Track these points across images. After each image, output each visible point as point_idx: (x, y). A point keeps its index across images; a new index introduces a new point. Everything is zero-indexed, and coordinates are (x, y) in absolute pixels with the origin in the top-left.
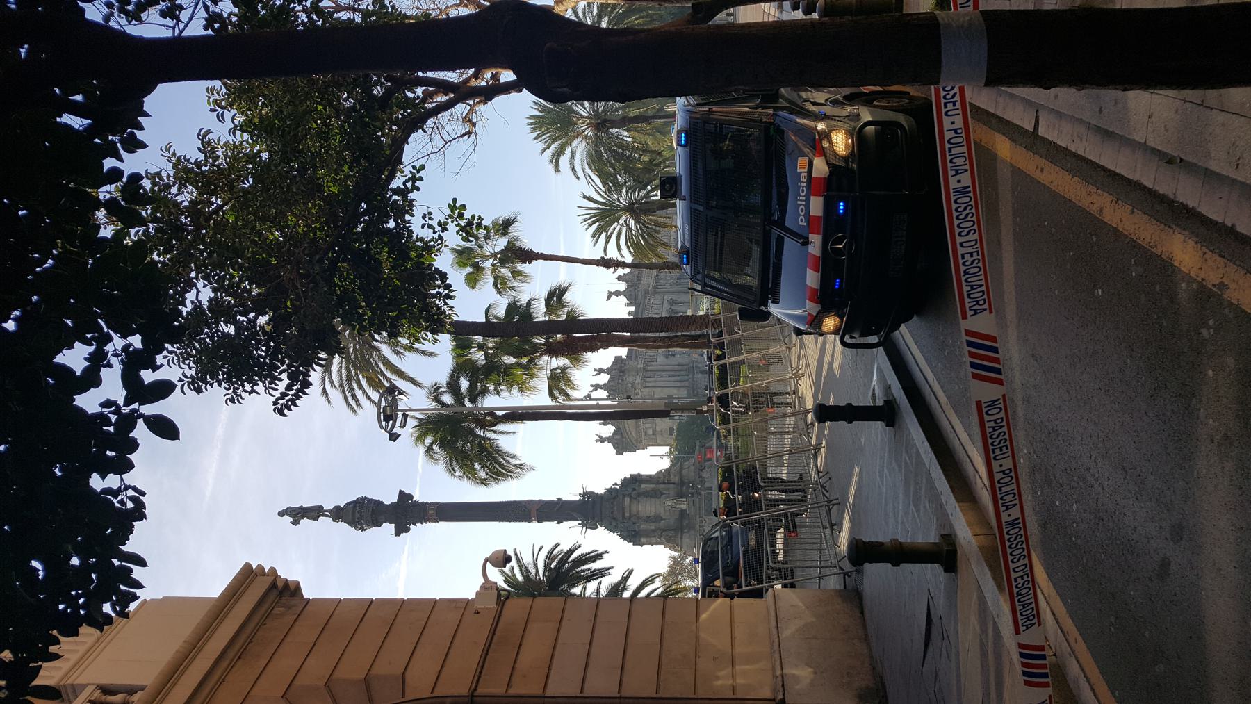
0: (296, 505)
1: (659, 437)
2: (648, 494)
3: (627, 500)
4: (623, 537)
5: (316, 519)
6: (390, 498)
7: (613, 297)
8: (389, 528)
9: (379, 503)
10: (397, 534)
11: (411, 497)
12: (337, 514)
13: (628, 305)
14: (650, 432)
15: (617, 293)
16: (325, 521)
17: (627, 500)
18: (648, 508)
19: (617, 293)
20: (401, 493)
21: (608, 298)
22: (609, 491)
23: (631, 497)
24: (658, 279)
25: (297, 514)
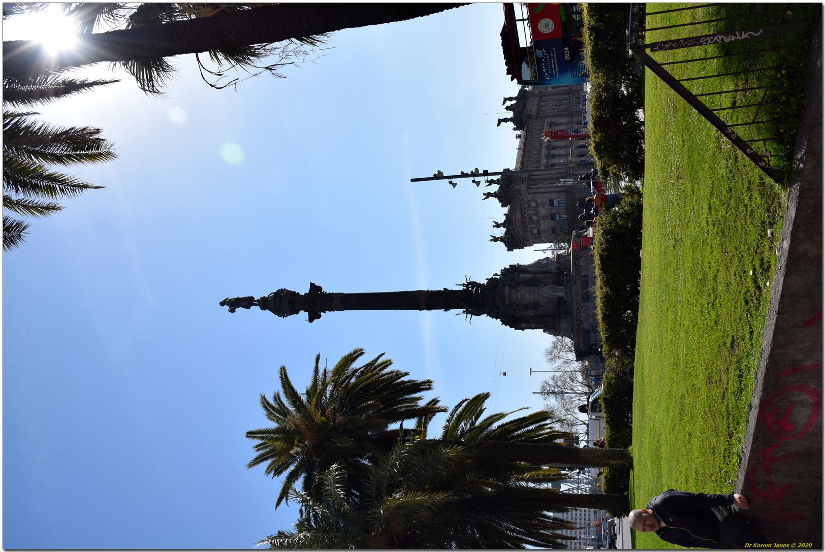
0: (233, 296)
1: (543, 235)
2: (526, 283)
3: (507, 289)
4: (505, 322)
5: (248, 307)
6: (303, 290)
7: (503, 123)
8: (304, 315)
9: (294, 294)
10: (311, 320)
11: (320, 288)
12: (264, 304)
13: (515, 129)
15: (506, 120)
16: (255, 309)
17: (507, 289)
18: (527, 296)
19: (506, 120)
20: (312, 285)
21: (499, 125)
22: (490, 280)
23: (511, 287)
24: (539, 106)
25: (234, 304)
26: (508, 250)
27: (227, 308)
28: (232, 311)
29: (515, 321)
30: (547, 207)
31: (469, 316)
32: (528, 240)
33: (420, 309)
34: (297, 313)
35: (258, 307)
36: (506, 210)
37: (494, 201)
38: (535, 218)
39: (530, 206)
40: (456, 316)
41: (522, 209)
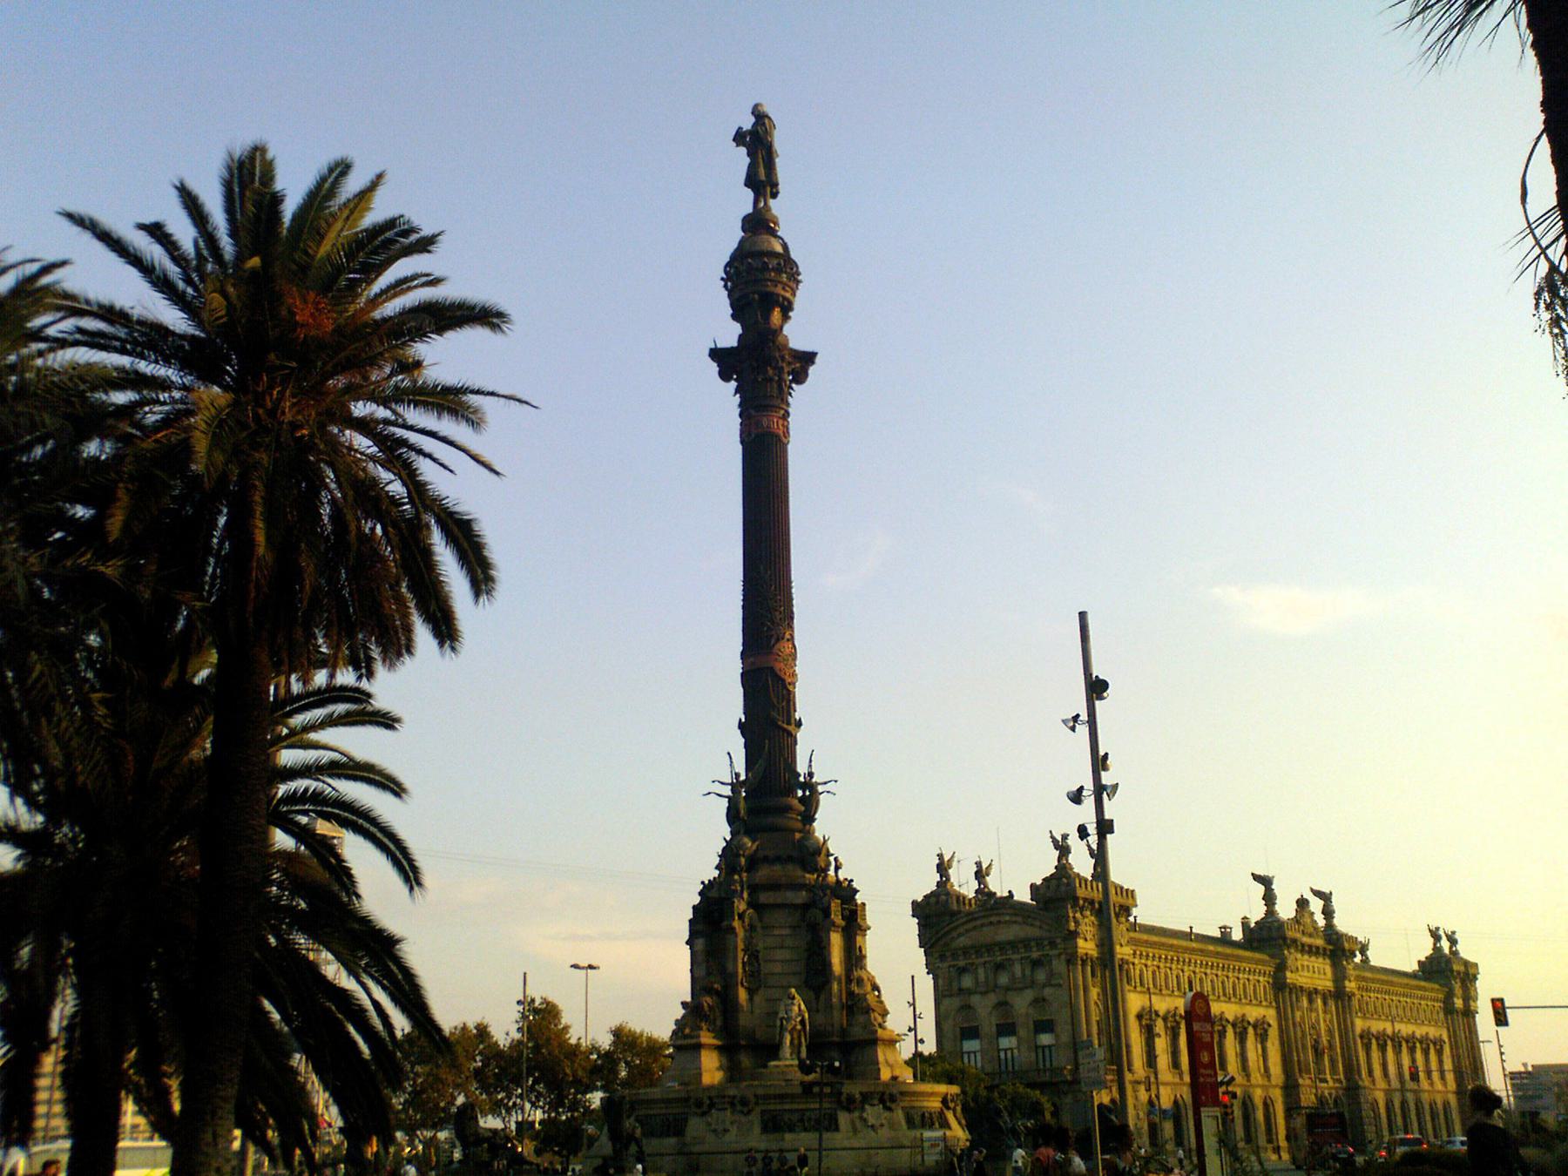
0: (780, 141)
1: (954, 1003)
4: (707, 889)
5: (752, 181)
6: (796, 334)
7: (1260, 889)
8: (729, 334)
10: (716, 354)
11: (800, 377)
12: (758, 224)
13: (1245, 923)
14: (967, 982)
15: (1269, 898)
16: (745, 201)
18: (780, 955)
19: (1269, 898)
20: (808, 358)
21: (1257, 878)
24: (1312, 994)
25: (757, 141)
26: (914, 903)
27: (748, 123)
28: (739, 138)
29: (710, 920)
31: (727, 791)
32: (942, 958)
33: (744, 655)
34: (734, 317)
35: (750, 210)
36: (1023, 895)
37: (1046, 865)
38: (1003, 979)
39: (1036, 964)
40: (724, 752)
41: (1026, 943)
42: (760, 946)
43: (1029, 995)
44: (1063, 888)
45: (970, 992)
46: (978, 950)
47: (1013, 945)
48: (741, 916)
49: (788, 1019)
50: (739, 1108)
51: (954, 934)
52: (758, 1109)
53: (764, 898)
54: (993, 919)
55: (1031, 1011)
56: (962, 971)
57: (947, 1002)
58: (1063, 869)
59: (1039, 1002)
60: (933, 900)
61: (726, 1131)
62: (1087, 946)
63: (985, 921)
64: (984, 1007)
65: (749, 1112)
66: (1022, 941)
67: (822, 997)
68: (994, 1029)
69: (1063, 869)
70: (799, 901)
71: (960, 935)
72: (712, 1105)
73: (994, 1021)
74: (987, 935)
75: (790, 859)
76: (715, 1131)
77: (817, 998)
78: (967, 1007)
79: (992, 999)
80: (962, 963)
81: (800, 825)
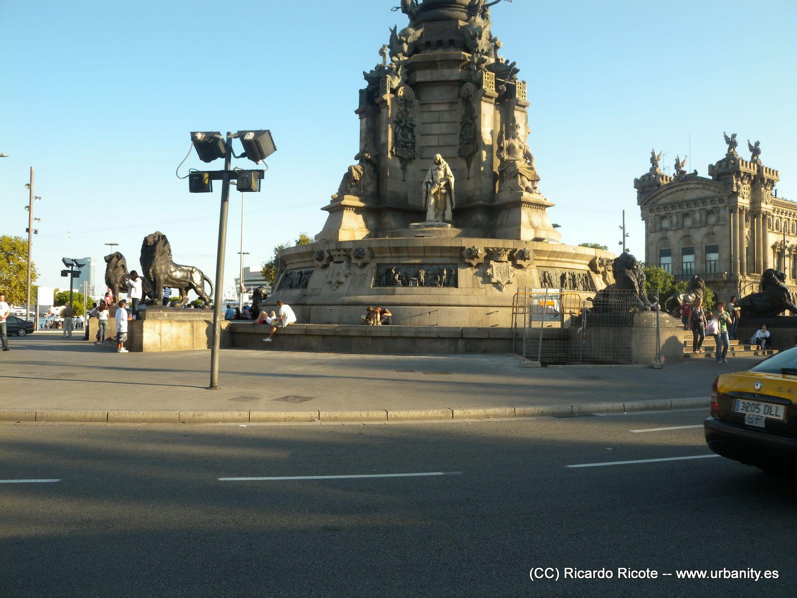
1: (659, 235)
14: (666, 224)
26: (636, 181)
30: (707, 242)
32: (651, 211)
36: (704, 173)
37: (720, 153)
38: (688, 222)
39: (709, 213)
41: (704, 200)
42: (417, 121)
43: (704, 231)
44: (730, 167)
45: (667, 230)
46: (673, 205)
47: (695, 202)
48: (394, 91)
49: (433, 184)
50: (354, 261)
51: (659, 197)
52: (373, 264)
53: (421, 76)
54: (684, 187)
55: (705, 240)
56: (663, 218)
57: (653, 235)
58: (731, 156)
59: (710, 234)
60: (647, 178)
61: (340, 283)
62: (744, 202)
63: (678, 188)
64: (675, 239)
65: (364, 265)
66: (701, 199)
67: (473, 165)
68: (681, 251)
69: (731, 156)
70: (455, 77)
71: (662, 197)
72: (331, 258)
73: (681, 246)
74: (679, 196)
75: (452, 43)
76: (330, 283)
77: (469, 166)
78: (665, 238)
79: (681, 233)
80: (663, 213)
81: (464, 15)
